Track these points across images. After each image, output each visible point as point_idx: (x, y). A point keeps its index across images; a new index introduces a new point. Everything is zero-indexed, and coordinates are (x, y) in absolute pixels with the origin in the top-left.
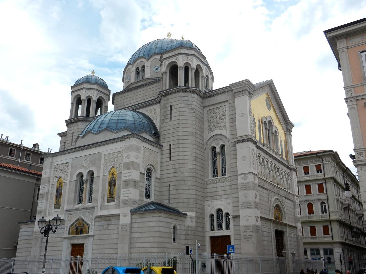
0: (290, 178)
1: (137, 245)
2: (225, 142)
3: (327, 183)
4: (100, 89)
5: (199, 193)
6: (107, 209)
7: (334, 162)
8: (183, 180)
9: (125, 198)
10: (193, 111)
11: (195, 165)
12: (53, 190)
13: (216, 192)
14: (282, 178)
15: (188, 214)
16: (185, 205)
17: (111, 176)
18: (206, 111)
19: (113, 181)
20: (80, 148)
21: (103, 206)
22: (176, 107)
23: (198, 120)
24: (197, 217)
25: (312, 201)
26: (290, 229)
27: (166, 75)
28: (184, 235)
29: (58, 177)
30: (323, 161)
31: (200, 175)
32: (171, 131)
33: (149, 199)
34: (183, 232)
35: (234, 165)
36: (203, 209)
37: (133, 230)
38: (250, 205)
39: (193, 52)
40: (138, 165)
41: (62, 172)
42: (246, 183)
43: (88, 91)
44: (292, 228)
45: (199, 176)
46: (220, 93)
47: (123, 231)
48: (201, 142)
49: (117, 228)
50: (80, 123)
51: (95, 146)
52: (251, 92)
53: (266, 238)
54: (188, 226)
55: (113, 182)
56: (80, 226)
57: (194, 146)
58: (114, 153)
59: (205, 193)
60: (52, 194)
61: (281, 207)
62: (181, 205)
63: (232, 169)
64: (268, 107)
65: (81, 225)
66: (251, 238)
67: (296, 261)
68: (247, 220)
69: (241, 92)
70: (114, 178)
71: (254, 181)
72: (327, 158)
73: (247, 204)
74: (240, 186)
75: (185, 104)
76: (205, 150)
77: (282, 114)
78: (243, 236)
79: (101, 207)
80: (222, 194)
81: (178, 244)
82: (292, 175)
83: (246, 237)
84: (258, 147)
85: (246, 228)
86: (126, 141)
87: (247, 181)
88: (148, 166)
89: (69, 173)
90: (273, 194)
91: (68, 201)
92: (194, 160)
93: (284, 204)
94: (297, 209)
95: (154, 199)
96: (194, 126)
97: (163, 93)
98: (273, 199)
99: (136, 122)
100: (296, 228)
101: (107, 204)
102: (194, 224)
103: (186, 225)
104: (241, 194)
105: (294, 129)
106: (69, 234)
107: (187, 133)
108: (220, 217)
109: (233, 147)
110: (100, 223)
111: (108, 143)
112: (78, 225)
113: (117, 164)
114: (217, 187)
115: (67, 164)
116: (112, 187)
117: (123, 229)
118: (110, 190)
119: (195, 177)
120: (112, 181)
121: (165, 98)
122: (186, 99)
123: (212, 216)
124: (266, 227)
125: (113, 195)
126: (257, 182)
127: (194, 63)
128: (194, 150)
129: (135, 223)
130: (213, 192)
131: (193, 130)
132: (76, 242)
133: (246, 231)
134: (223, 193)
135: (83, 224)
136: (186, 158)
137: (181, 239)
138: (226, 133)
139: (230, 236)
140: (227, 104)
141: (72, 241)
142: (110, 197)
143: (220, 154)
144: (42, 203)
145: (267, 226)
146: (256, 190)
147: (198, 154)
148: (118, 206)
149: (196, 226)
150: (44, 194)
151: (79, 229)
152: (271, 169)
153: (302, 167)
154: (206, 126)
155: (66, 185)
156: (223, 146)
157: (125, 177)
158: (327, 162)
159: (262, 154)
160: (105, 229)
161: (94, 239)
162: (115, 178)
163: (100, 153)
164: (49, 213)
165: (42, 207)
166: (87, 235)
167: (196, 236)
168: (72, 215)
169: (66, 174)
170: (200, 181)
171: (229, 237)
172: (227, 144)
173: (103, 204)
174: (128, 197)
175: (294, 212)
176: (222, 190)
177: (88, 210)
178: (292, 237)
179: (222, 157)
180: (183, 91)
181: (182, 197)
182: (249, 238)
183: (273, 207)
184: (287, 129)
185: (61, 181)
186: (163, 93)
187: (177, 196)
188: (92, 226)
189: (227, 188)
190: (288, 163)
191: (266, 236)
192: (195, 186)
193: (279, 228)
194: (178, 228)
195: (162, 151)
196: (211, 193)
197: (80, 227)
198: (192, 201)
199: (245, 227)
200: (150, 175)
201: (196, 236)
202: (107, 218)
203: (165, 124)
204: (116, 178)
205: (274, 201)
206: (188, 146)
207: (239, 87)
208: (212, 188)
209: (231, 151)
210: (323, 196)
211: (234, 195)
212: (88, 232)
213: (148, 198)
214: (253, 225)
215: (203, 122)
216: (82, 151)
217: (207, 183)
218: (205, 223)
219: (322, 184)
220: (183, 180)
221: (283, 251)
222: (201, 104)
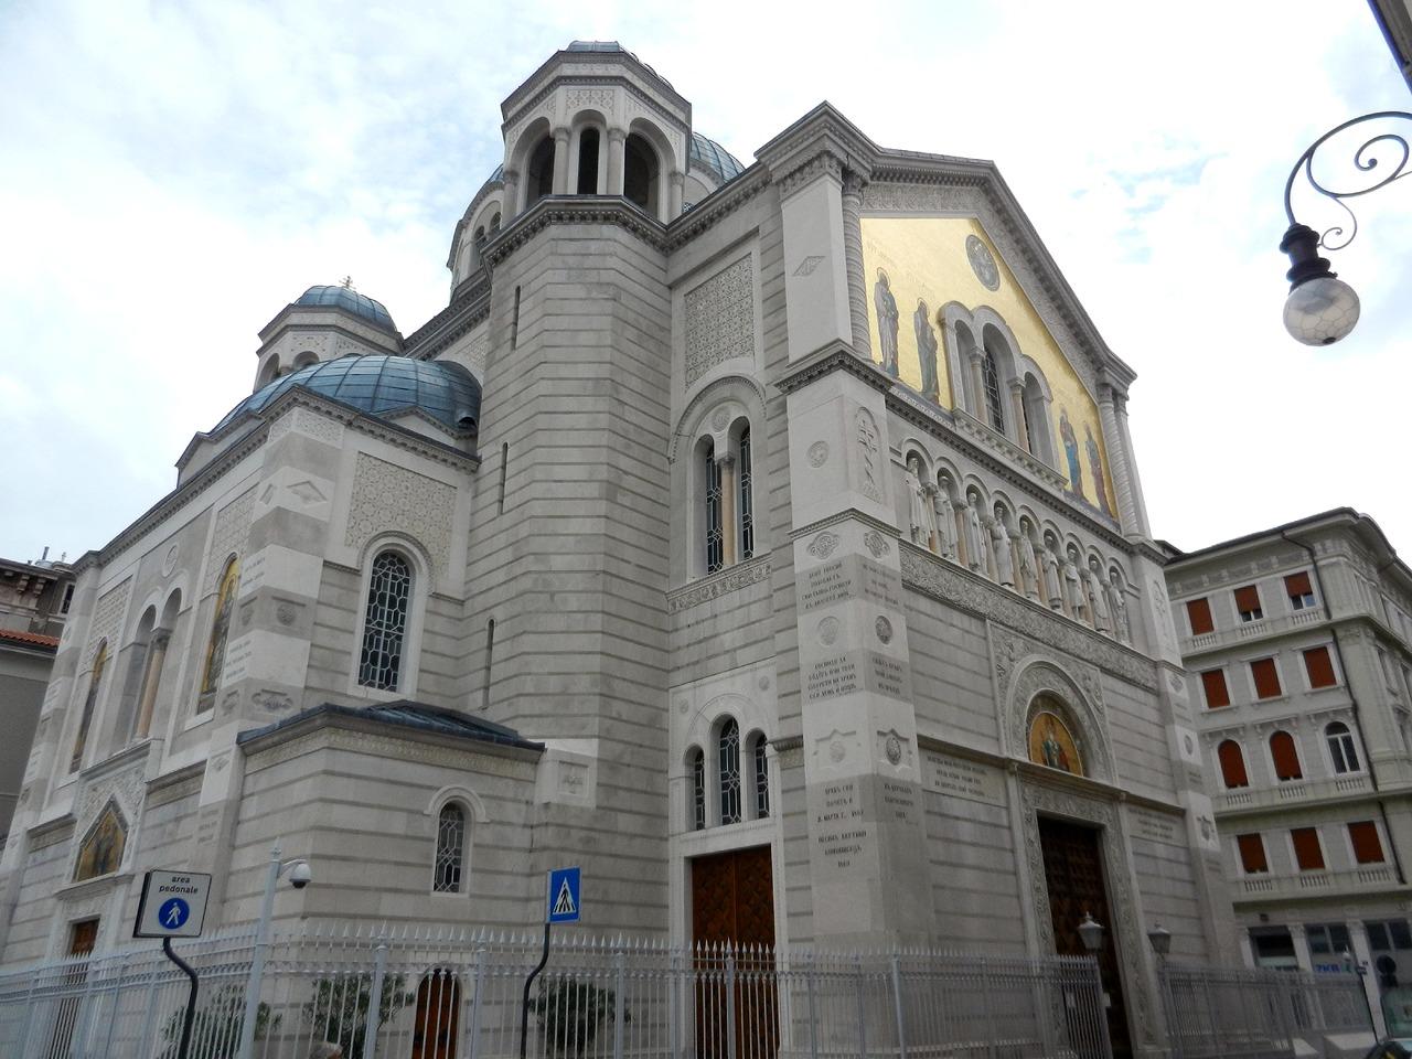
0: (1130, 585)
2: (745, 406)
3: (1342, 644)
4: (351, 326)
5: (630, 651)
7: (1366, 560)
8: (541, 592)
10: (605, 293)
11: (603, 520)
13: (712, 637)
14: (1078, 578)
15: (550, 744)
16: (545, 706)
18: (678, 299)
22: (535, 286)
23: (631, 333)
24: (608, 764)
25: (1288, 721)
26: (1143, 818)
27: (515, 185)
28: (519, 849)
30: (1316, 558)
31: (638, 566)
32: (512, 390)
33: (393, 689)
34: (521, 838)
35: (780, 498)
36: (655, 723)
37: (246, 832)
38: (850, 672)
39: (615, 70)
40: (319, 530)
42: (827, 570)
43: (303, 336)
44: (1154, 813)
45: (628, 571)
46: (729, 208)
48: (651, 425)
52: (853, 166)
53: (971, 855)
54: (547, 805)
57: (605, 438)
59: (667, 652)
61: (1079, 711)
62: (525, 705)
63: (775, 519)
64: (980, 275)
67: (1186, 977)
68: (839, 756)
69: (807, 169)
71: (868, 554)
72: (1328, 543)
73: (837, 671)
74: (802, 589)
75: (570, 269)
76: (671, 461)
77: (1064, 317)
78: (821, 840)
81: (472, 896)
82: (1138, 575)
83: (837, 849)
84: (894, 405)
85: (832, 797)
87: (835, 556)
88: (383, 541)
89: (123, 621)
90: (1019, 644)
91: (101, 734)
92: (601, 499)
93: (1099, 698)
94: (1177, 728)
95: (418, 690)
96: (607, 355)
97: (494, 249)
98: (1020, 667)
99: (385, 381)
100: (1180, 813)
101: (193, 721)
102: (586, 796)
103: (537, 801)
104: (807, 622)
105: (1133, 390)
107: (566, 387)
108: (727, 758)
109: (777, 420)
114: (716, 616)
119: (604, 572)
121: (502, 268)
122: (574, 246)
123: (696, 755)
124: (975, 797)
126: (892, 558)
127: (621, 112)
128: (603, 456)
130: (700, 642)
131: (604, 371)
132: (83, 912)
136: (562, 490)
137: (502, 873)
138: (752, 366)
139: (770, 845)
140: (754, 247)
143: (730, 462)
145: (981, 794)
146: (883, 601)
147: (626, 473)
149: (598, 807)
151: (104, 847)
152: (1002, 530)
153: (1227, 593)
154: (678, 362)
156: (742, 431)
158: (1334, 560)
159: (937, 449)
167: (596, 854)
168: (94, 790)
170: (638, 594)
171: (763, 852)
172: (754, 412)
175: (1166, 743)
176: (736, 626)
178: (1155, 858)
179: (744, 478)
180: (560, 218)
181: (534, 670)
182: (844, 850)
183: (1021, 700)
184: (1103, 386)
186: (494, 249)
187: (512, 667)
189: (756, 611)
190: (1118, 526)
191: (973, 844)
192: (603, 612)
193: (1070, 808)
194: (479, 811)
195: (477, 480)
196: (691, 648)
198: (583, 684)
199: (827, 792)
200: (407, 581)
201: (596, 854)
203: (495, 367)
205: (1027, 672)
206: (575, 438)
207: (794, 152)
208: (697, 623)
209: (769, 438)
210: (1333, 700)
211: (782, 641)
213: (381, 687)
214: (863, 779)
215: (664, 347)
217: (678, 605)
218: (667, 796)
219: (1323, 650)
220: (541, 592)
221: (1084, 921)
222: (660, 275)
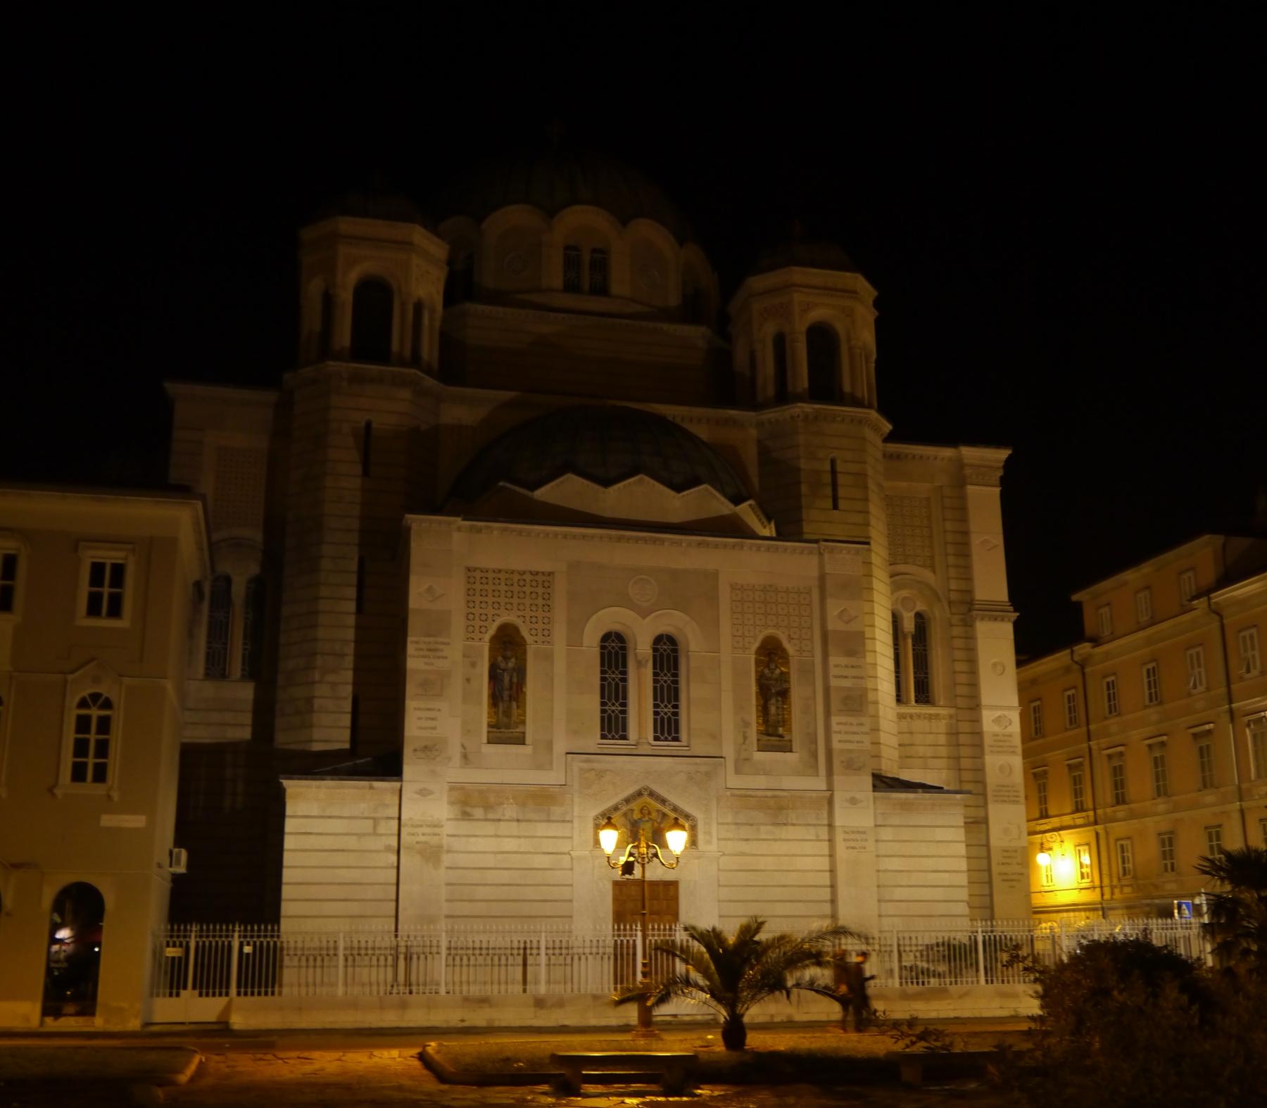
1: (899, 893)
6: (766, 773)
9: (849, 746)
12: (473, 665)
19: (777, 680)
21: (747, 760)
42: (1004, 735)
47: (853, 848)
49: (814, 838)
50: (406, 394)
56: (647, 819)
60: (468, 680)
66: (1019, 881)
74: (988, 741)
79: (736, 761)
80: (929, 755)
85: (1006, 854)
112: (636, 816)
116: (773, 701)
117: (852, 844)
129: (884, 826)
133: (1004, 861)
134: (929, 752)
142: (769, 735)
148: (811, 767)
163: (712, 577)
164: (465, 757)
165: (434, 728)
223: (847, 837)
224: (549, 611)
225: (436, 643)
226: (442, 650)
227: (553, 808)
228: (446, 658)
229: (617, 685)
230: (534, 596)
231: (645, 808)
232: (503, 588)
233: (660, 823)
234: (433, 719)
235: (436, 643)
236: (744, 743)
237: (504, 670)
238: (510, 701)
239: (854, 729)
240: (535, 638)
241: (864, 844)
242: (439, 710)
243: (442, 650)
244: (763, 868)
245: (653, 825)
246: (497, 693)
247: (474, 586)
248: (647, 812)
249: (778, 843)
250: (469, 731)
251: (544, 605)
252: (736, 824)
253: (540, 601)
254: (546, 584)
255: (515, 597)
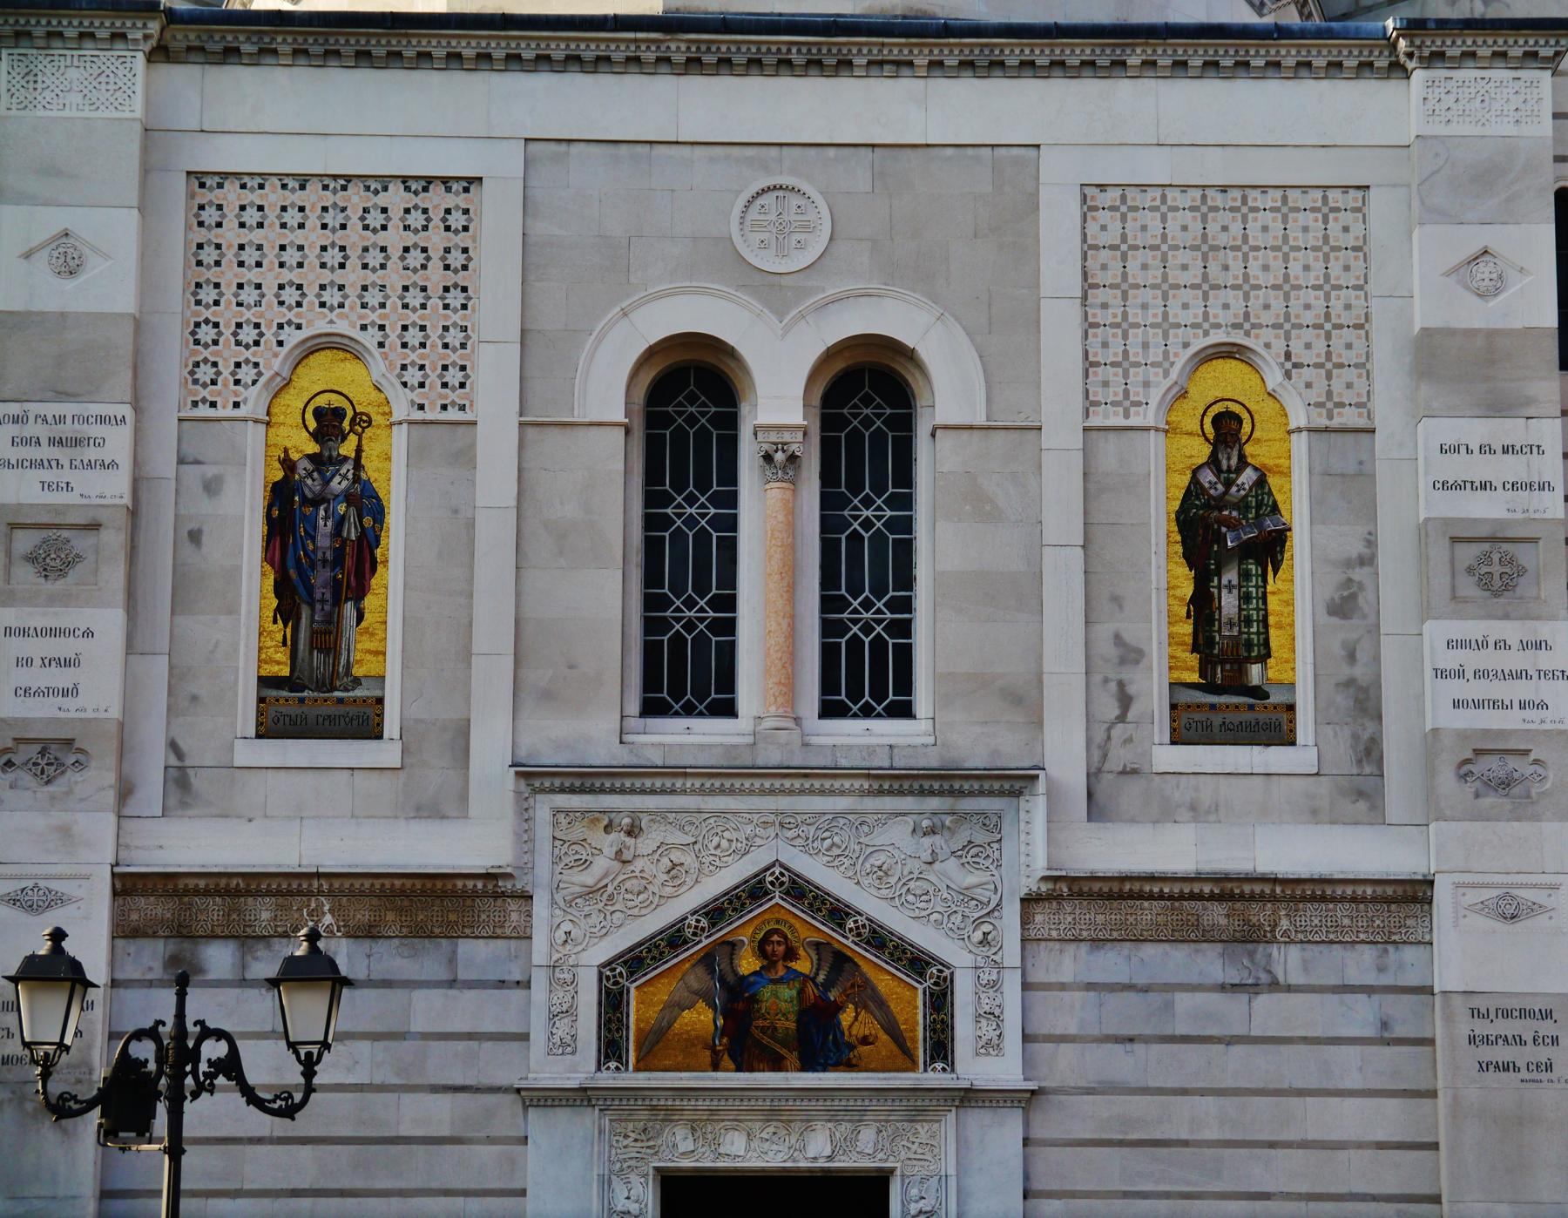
6: (1196, 811)
12: (212, 487)
17: (1202, 451)
19: (1242, 505)
20: (678, 47)
21: (1130, 772)
29: (292, 337)
41: (353, 276)
49: (1369, 1032)
51: (921, 61)
55: (1233, 526)
58: (1224, 189)
60: (195, 537)
65: (803, 966)
70: (1248, 477)
79: (1093, 776)
86: (1430, 85)
106: (610, 1049)
110: (1112, 964)
111: (1134, 61)
112: (748, 964)
113: (1286, 325)
115: (437, 199)
116: (1231, 575)
117: (1501, 1053)
118: (1202, 606)
120: (1220, 503)
125: (1255, 670)
135: (840, 962)
141: (688, 1145)
142: (1209, 687)
144: (53, 632)
150: (94, 527)
155: (466, 458)
157: (1456, 486)
160: (1181, 1030)
161: (1038, 1133)
162: (1261, 482)
164: (180, 781)
166: (934, 1078)
168: (629, 833)
169: (435, 317)
173: (1120, 756)
174: (1529, 714)
177: (908, 803)
185: (337, 401)
188: (994, 985)
197: (787, 993)
202: (1216, 914)
204: (1273, 481)
212: (941, 1049)
216: (696, 84)
223: (1483, 1027)
224: (464, 307)
225: (86, 420)
226: (100, 443)
227: (466, 947)
228: (113, 464)
229: (702, 538)
230: (415, 258)
231: (775, 938)
232: (313, 237)
233: (828, 985)
234: (67, 663)
235: (86, 420)
236: (1122, 718)
237: (316, 502)
238: (337, 602)
239: (1514, 660)
240: (417, 396)
241: (1543, 1053)
242: (89, 633)
243: (100, 443)
244: (1184, 1136)
245: (801, 992)
246: (293, 573)
247: (214, 235)
248: (782, 948)
249: (1238, 1050)
250: (194, 698)
251: (446, 289)
252: (1090, 987)
253: (435, 276)
254: (457, 220)
255: (354, 263)
